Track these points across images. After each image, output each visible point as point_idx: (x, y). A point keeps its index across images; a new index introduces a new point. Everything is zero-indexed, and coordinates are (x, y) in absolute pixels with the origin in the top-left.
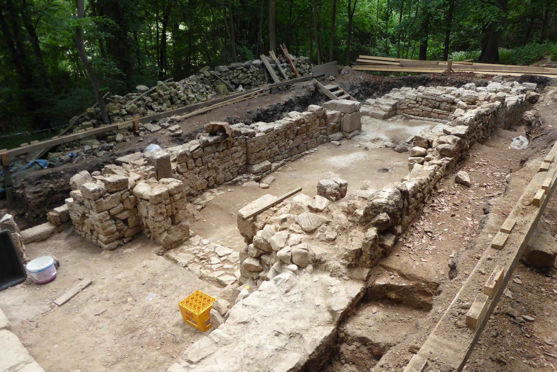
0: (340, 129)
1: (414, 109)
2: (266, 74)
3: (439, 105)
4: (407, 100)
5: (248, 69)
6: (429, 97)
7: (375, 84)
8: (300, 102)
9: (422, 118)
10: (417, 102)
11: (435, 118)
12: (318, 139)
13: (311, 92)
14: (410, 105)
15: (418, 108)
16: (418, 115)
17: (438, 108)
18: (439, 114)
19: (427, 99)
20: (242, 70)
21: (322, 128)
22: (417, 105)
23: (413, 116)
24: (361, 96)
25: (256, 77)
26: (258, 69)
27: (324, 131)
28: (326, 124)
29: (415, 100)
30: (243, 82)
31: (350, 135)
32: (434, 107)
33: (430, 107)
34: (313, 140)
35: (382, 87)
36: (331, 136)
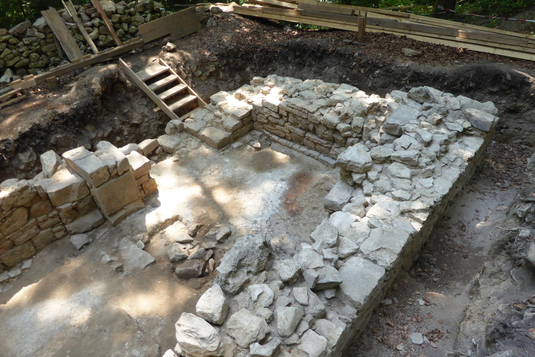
0: (93, 205)
1: (278, 127)
2: (56, 44)
3: (314, 129)
4: (265, 110)
5: (21, 40)
6: (296, 112)
7: (247, 53)
8: (66, 123)
9: (291, 144)
10: (281, 116)
11: (310, 148)
12: (36, 241)
13: (96, 95)
14: (270, 119)
15: (284, 126)
16: (285, 138)
17: (314, 132)
18: (316, 144)
19: (295, 116)
20: (6, 41)
21: (40, 219)
22: (281, 122)
23: (276, 138)
24: (221, 75)
25: (40, 52)
26: (42, 36)
27: (50, 221)
28: (53, 207)
29: (278, 113)
30: (11, 63)
31: (113, 220)
32: (307, 130)
33: (301, 128)
34: (17, 248)
35: (257, 57)
36: (69, 226)
